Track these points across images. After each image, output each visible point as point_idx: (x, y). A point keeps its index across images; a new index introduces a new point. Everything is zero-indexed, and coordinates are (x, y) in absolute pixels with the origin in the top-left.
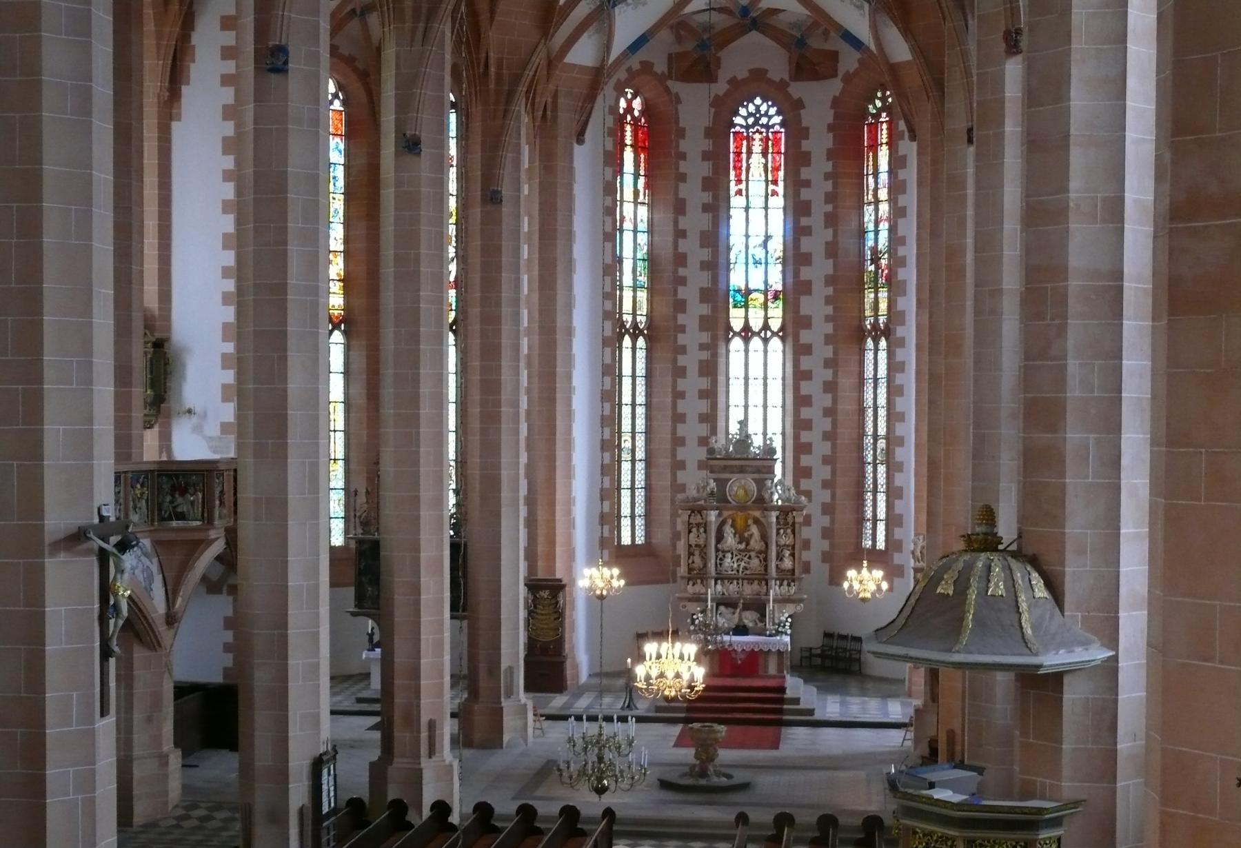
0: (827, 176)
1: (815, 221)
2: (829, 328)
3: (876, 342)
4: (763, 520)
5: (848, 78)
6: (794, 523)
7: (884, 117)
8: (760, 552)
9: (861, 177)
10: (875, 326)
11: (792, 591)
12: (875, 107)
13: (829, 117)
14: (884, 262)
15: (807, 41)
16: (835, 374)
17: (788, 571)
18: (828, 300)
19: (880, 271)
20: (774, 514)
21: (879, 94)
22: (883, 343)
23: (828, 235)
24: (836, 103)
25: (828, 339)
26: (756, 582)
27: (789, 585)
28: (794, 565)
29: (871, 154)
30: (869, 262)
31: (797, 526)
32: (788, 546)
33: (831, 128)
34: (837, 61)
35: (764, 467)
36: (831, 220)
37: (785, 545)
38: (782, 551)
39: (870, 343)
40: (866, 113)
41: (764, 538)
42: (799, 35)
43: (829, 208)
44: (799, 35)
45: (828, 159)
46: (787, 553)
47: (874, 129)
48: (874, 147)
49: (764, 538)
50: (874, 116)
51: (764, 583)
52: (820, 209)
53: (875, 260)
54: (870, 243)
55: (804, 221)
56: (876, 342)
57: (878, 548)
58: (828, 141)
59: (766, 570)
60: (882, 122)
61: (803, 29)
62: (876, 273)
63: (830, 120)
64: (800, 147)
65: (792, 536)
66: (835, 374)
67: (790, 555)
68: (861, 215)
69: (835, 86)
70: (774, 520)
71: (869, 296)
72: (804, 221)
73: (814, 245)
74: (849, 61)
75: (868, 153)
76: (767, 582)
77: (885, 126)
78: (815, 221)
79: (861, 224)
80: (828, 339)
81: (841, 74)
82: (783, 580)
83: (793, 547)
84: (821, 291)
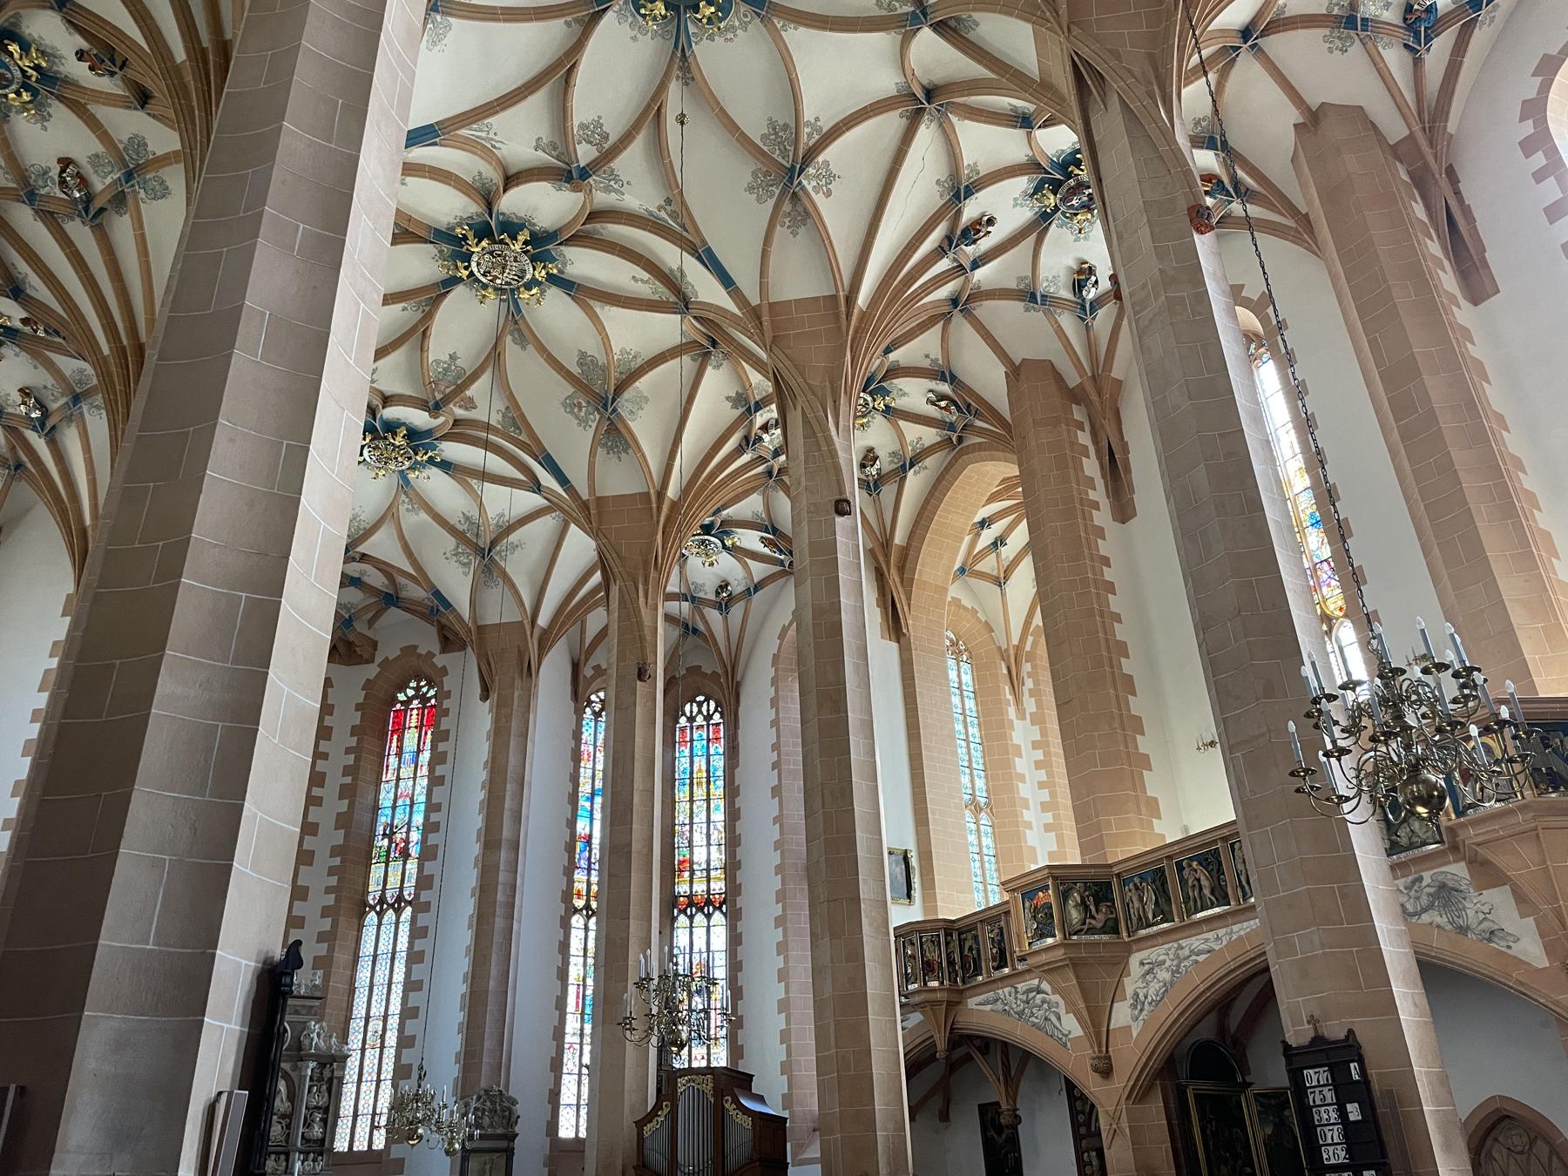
0: (348, 751)
1: (329, 792)
2: (330, 900)
3: (380, 915)
4: (293, 1074)
5: (385, 663)
6: (331, 1080)
7: (415, 703)
8: (283, 1116)
9: (381, 757)
10: (382, 900)
11: (318, 1169)
12: (406, 695)
13: (360, 697)
14: (398, 837)
15: (354, 624)
16: (331, 949)
17: (315, 1141)
18: (332, 871)
19: (394, 845)
20: (312, 1065)
21: (413, 684)
22: (390, 915)
23: (343, 805)
24: (368, 685)
25: (326, 912)
26: (273, 1157)
27: (314, 1161)
28: (324, 1133)
29: (395, 737)
30: (380, 837)
31: (335, 1081)
32: (320, 1108)
33: (358, 707)
34: (375, 649)
35: (303, 1006)
36: (347, 792)
37: (316, 1107)
38: (311, 1115)
39: (372, 917)
40: (395, 700)
41: (292, 1096)
42: (347, 616)
43: (348, 780)
44: (347, 616)
45: (352, 735)
46: (318, 1117)
47: (401, 717)
48: (400, 730)
49: (292, 1096)
50: (402, 703)
51: (283, 1157)
52: (335, 780)
53: (390, 835)
54: (383, 819)
55: (316, 791)
56: (380, 915)
57: (355, 1149)
58: (356, 719)
59: (287, 1141)
60: (413, 709)
61: (353, 611)
62: (389, 847)
63: (361, 700)
64: (421, 655)
65: (326, 1094)
66: (331, 949)
67: (321, 1120)
68: (378, 792)
69: (371, 671)
70: (309, 1072)
71: (377, 872)
72: (316, 791)
73: (325, 816)
74: (389, 650)
75: (392, 736)
76: (287, 1155)
77: (415, 712)
78: (329, 792)
79: (376, 800)
80: (326, 912)
81: (379, 659)
82: (308, 1153)
83: (326, 1110)
84: (324, 860)
